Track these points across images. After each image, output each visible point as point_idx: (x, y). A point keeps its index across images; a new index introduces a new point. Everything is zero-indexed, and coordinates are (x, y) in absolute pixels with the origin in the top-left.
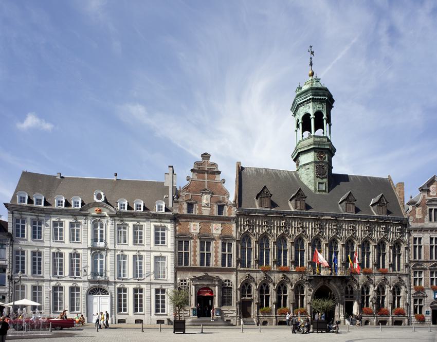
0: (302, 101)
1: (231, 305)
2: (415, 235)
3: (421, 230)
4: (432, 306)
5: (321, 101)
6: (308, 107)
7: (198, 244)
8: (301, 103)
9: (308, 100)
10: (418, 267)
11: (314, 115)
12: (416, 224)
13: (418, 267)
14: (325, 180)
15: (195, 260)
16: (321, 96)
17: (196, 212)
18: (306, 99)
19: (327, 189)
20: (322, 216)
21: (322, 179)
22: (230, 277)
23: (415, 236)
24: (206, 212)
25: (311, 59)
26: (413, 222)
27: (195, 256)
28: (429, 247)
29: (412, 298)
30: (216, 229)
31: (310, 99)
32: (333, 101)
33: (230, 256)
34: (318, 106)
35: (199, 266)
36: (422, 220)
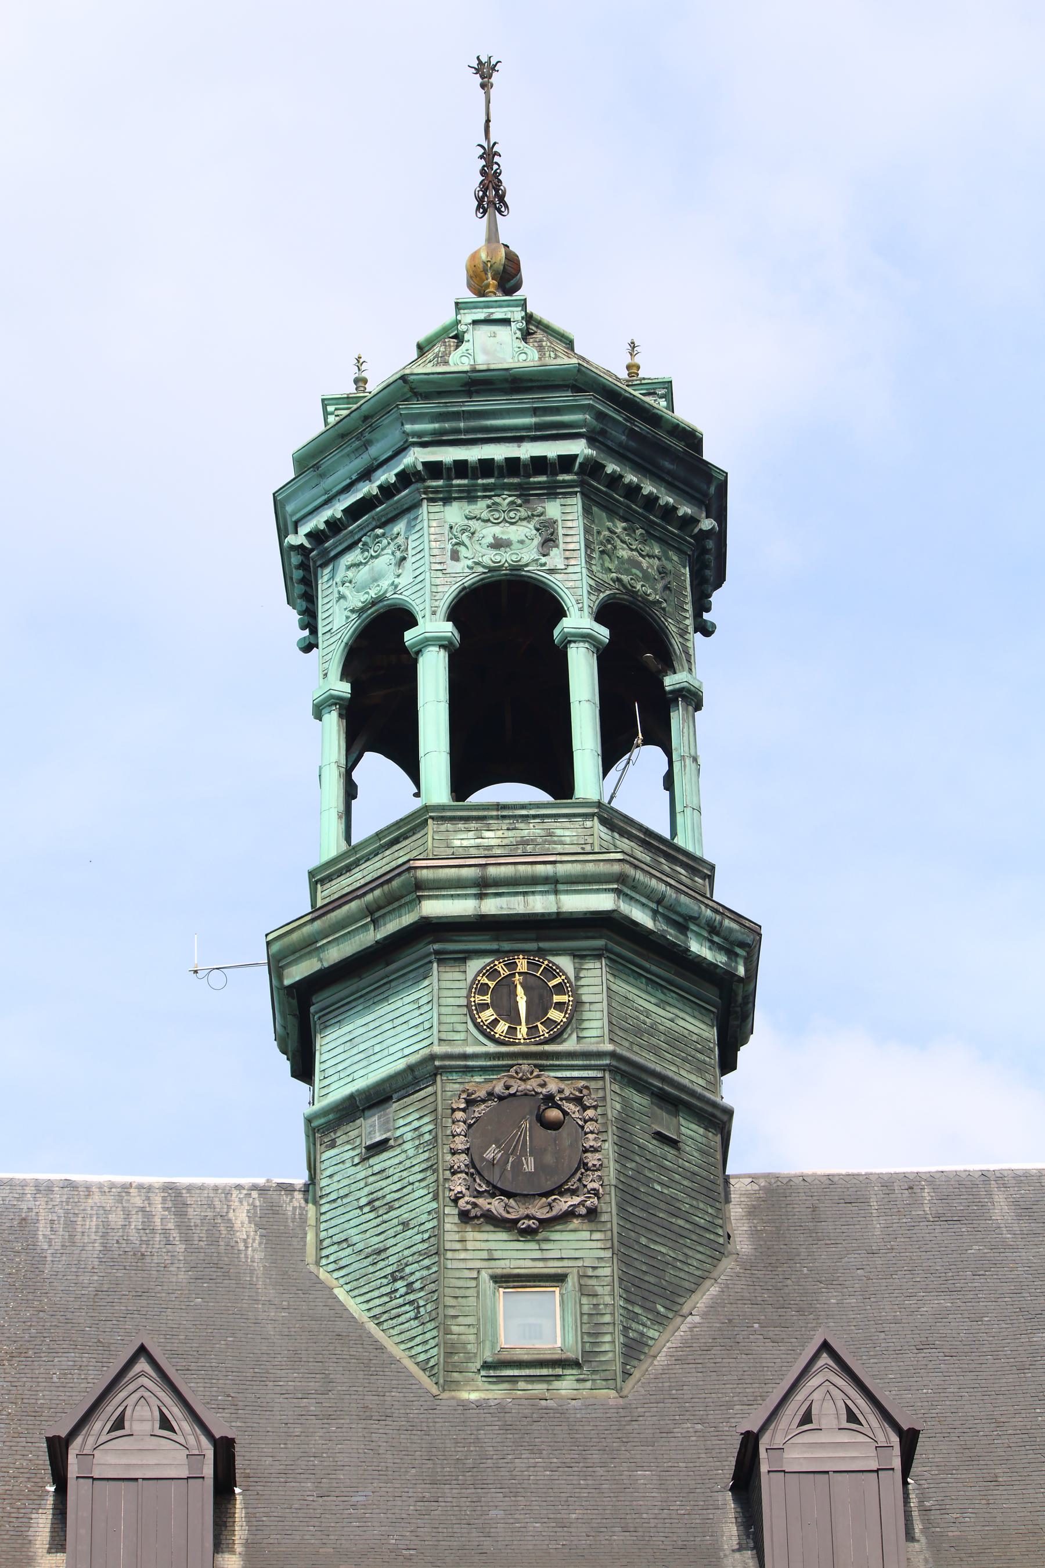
5: (527, 482)
6: (384, 562)
8: (334, 526)
9: (387, 491)
11: (456, 613)
14: (578, 1246)
19: (610, 1345)
25: (489, 155)
32: (709, 488)
34: (490, 532)
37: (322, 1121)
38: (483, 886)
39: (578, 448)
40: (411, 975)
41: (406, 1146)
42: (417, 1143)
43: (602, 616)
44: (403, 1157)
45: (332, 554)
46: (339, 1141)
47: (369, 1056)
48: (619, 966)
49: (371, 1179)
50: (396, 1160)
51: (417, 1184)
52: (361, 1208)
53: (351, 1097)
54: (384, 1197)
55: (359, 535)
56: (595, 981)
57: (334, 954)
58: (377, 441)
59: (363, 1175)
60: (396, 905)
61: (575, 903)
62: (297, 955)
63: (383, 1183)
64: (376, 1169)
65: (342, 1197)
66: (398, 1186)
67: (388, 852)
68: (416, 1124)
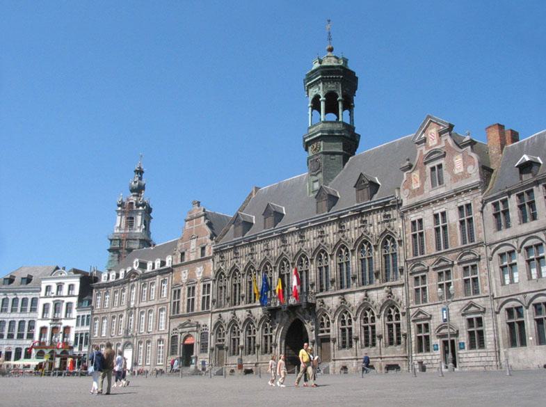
1: (206, 352)
2: (413, 216)
3: (418, 206)
4: (438, 334)
7: (187, 290)
10: (416, 269)
12: (413, 198)
13: (416, 269)
15: (183, 308)
17: (186, 260)
20: (286, 229)
21: (316, 175)
22: (207, 321)
23: (413, 219)
24: (193, 258)
26: (409, 197)
27: (184, 303)
28: (433, 230)
29: (412, 323)
30: (199, 272)
33: (208, 297)
35: (186, 313)
36: (420, 191)
38: (310, 136)
39: (320, 76)
43: (325, 97)
48: (325, 141)
56: (322, 143)
61: (318, 135)
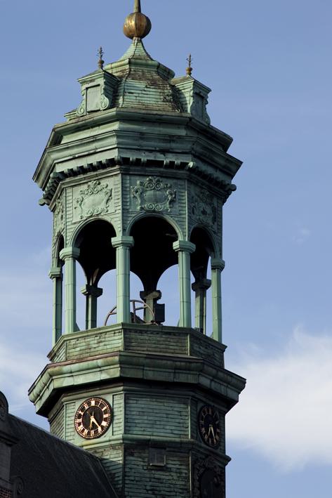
0: (144, 157)
11: (193, 237)
16: (216, 168)
18: (160, 157)
31: (184, 165)
34: (202, 205)
37: (129, 442)
40: (177, 399)
41: (172, 474)
42: (179, 475)
44: (170, 478)
45: (131, 173)
46: (135, 455)
47: (153, 424)
49: (153, 480)
50: (167, 478)
51: (178, 494)
52: (147, 490)
53: (149, 440)
54: (160, 491)
55: (149, 174)
57: (150, 375)
58: (177, 143)
59: (148, 476)
60: (188, 372)
62: (131, 366)
63: (160, 485)
64: (156, 476)
65: (137, 481)
66: (168, 489)
67: (164, 336)
68: (180, 467)
